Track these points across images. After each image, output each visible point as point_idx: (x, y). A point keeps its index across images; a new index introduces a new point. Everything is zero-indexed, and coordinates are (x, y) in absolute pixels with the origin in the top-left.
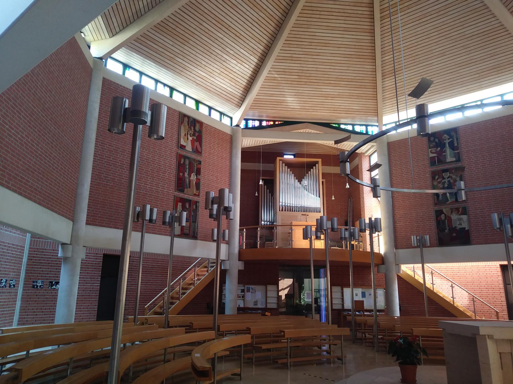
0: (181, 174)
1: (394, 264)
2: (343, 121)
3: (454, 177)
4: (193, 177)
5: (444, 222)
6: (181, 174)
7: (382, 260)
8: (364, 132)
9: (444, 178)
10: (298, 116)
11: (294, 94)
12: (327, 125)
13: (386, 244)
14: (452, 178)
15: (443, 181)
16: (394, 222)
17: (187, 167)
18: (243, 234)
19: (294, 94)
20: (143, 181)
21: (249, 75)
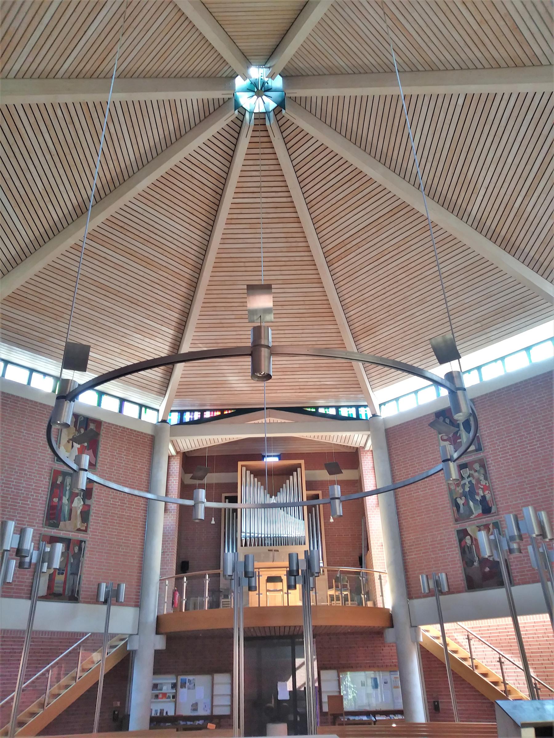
0: (56, 500)
2: (321, 402)
6: (56, 500)
7: (390, 619)
8: (355, 416)
10: (253, 401)
11: (237, 371)
13: (392, 591)
14: (474, 478)
18: (183, 585)
19: (237, 371)
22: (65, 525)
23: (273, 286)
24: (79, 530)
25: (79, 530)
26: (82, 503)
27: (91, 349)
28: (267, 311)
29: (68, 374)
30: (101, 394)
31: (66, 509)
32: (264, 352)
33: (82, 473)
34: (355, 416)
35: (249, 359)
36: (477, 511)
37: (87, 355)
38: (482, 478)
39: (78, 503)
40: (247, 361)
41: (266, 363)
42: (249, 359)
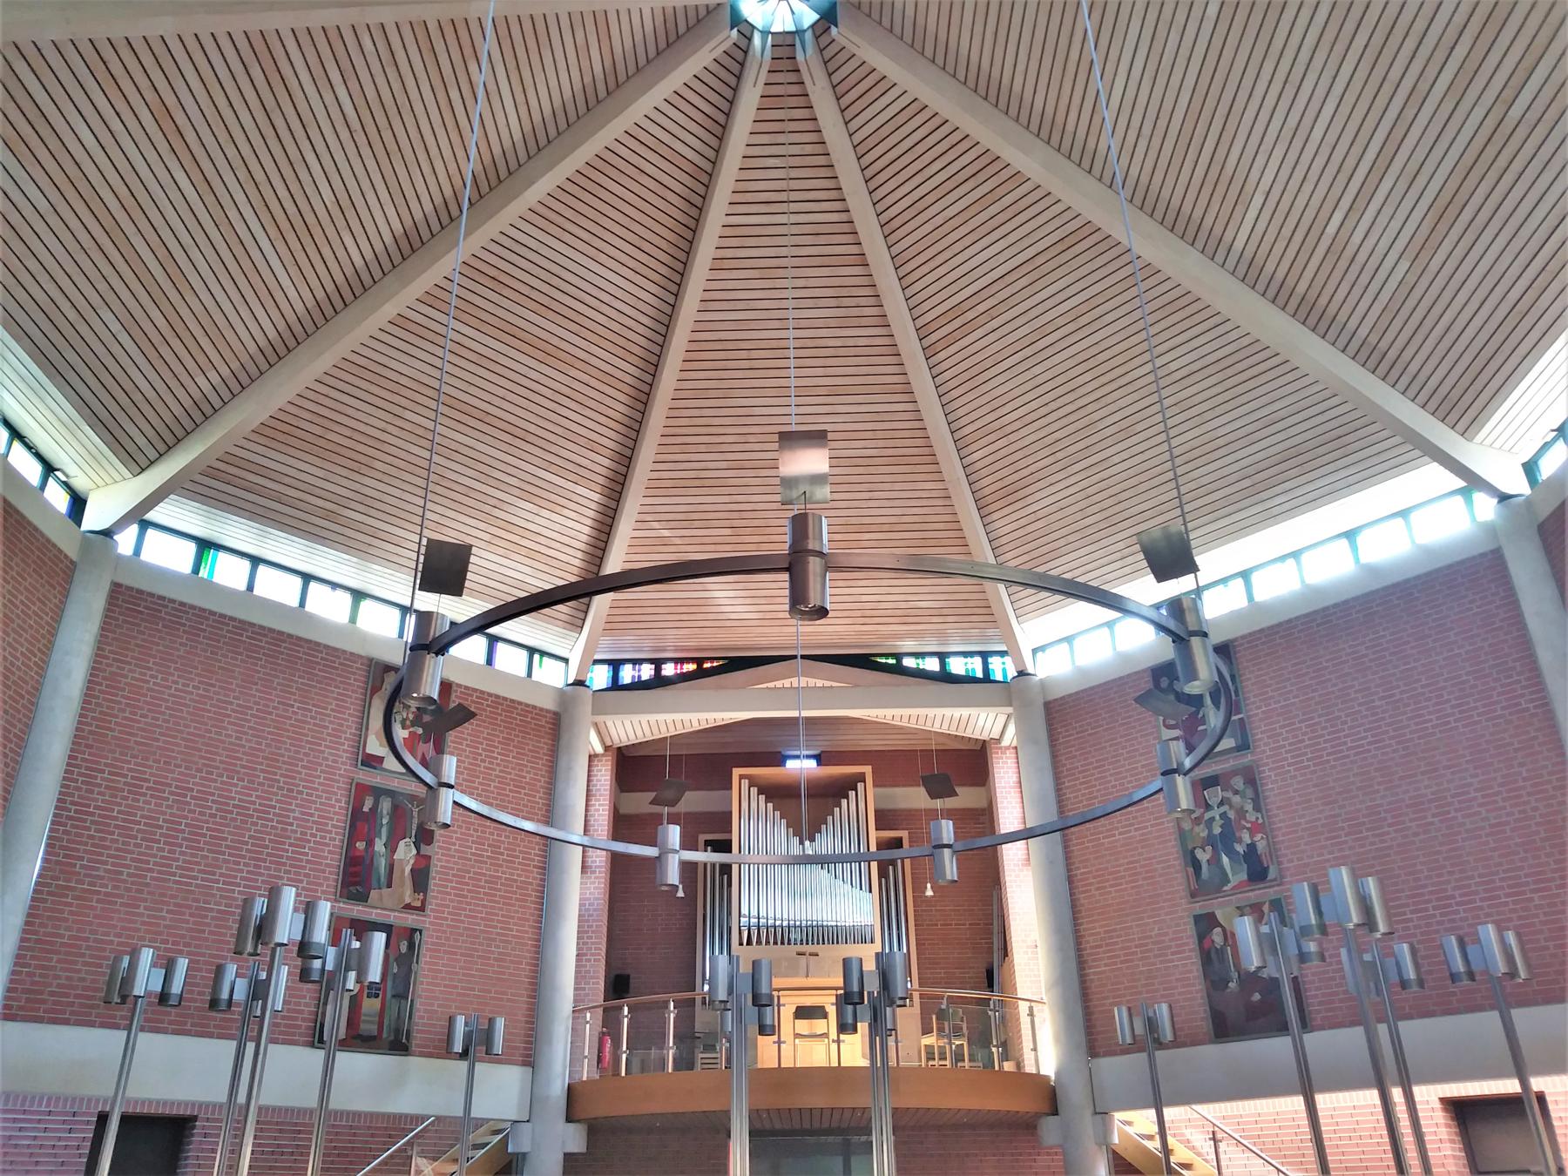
0: (361, 845)
1: (1088, 1112)
2: (908, 645)
3: (1236, 799)
4: (406, 852)
5: (1221, 952)
6: (361, 845)
7: (1050, 1097)
8: (980, 674)
9: (1208, 807)
10: (763, 642)
12: (863, 661)
13: (1057, 1040)
14: (1231, 807)
15: (1207, 816)
16: (1081, 964)
17: (385, 821)
18: (620, 1023)
20: (221, 875)
21: (585, 538)
22: (381, 898)
23: (830, 436)
24: (408, 907)
25: (408, 907)
26: (414, 852)
27: (474, 550)
28: (818, 479)
29: (428, 601)
30: (494, 640)
31: (382, 863)
32: (814, 564)
33: (444, 790)
34: (980, 674)
35: (786, 576)
36: (1237, 875)
37: (467, 562)
38: (1249, 807)
39: (406, 852)
40: (780, 583)
41: (819, 587)
42: (786, 576)
